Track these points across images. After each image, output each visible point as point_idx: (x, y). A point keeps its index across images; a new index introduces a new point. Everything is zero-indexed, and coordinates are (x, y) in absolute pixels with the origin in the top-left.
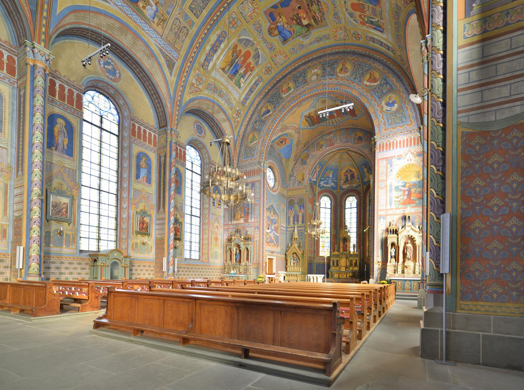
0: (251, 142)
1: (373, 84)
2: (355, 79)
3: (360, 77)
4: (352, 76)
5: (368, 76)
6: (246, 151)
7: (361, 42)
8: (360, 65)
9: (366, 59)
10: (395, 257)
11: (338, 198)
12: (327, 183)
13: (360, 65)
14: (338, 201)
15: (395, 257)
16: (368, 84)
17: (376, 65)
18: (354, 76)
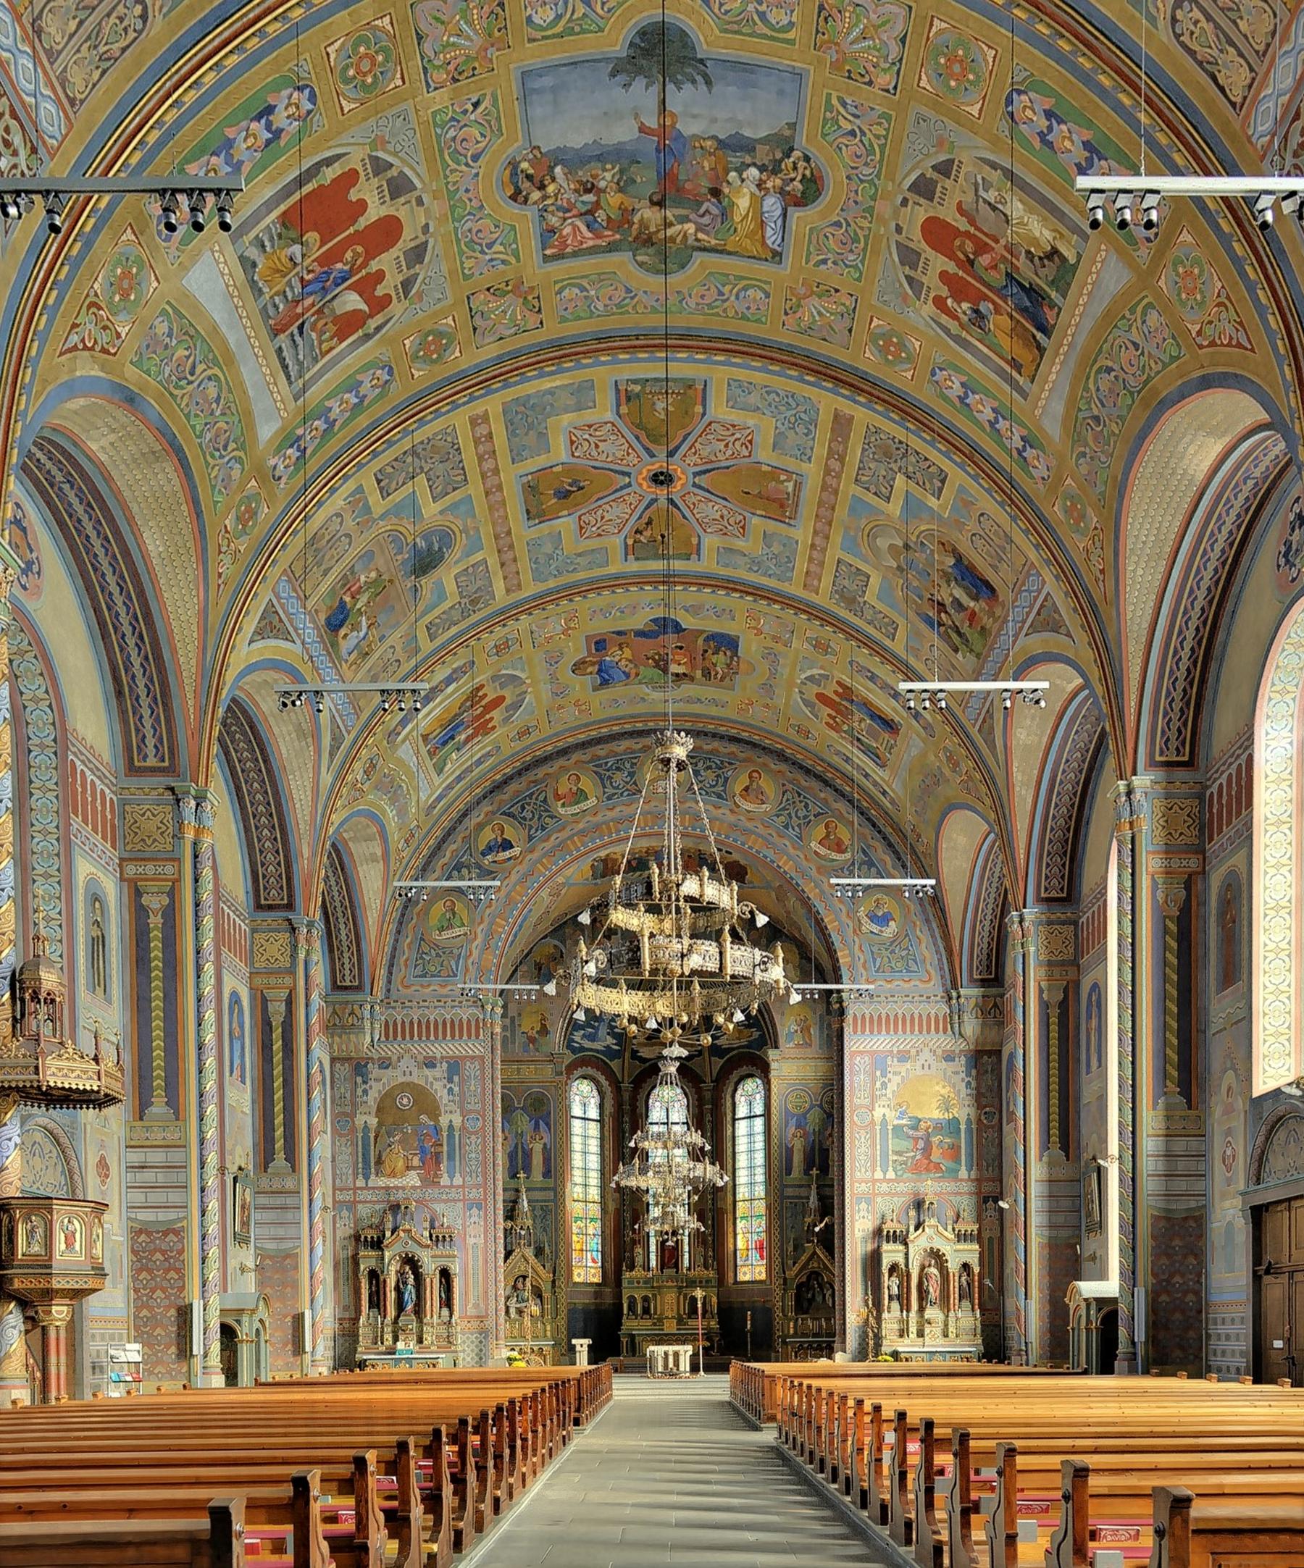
0: (442, 929)
1: (834, 856)
2: (786, 827)
3: (799, 826)
4: (778, 816)
5: (820, 831)
6: (421, 954)
7: (810, 743)
8: (799, 795)
9: (815, 784)
10: (899, 1297)
11: (626, 1085)
12: (592, 1038)
13: (799, 795)
14: (626, 1096)
15: (899, 1297)
16: (823, 851)
17: (841, 806)
18: (782, 819)
